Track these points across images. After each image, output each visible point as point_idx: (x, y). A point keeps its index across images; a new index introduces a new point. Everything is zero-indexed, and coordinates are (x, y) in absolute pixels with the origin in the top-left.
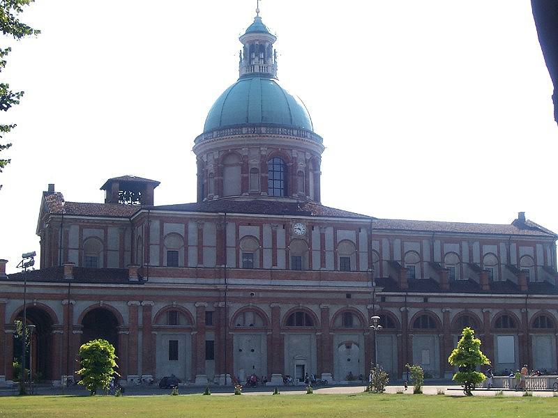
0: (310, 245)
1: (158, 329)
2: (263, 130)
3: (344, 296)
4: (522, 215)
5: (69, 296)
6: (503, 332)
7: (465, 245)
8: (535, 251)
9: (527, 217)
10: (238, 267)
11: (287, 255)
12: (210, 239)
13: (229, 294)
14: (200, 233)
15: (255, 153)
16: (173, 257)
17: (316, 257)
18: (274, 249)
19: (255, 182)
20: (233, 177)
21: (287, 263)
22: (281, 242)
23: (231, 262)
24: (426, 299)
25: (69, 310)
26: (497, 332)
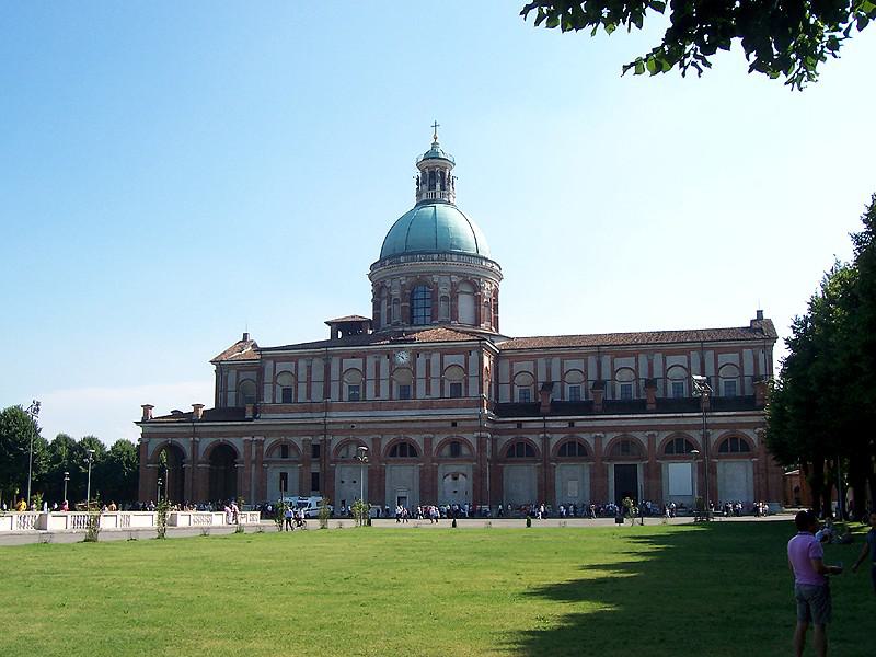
0: (414, 373)
1: (267, 462)
2: (402, 259)
3: (450, 425)
4: (760, 313)
5: (194, 435)
6: (674, 458)
7: (541, 362)
8: (741, 359)
9: (766, 316)
10: (341, 400)
11: (391, 386)
12: (318, 374)
13: (329, 427)
14: (309, 368)
15: (396, 283)
16: (287, 395)
17: (421, 385)
18: (378, 381)
19: (397, 310)
20: (384, 310)
21: (391, 393)
22: (385, 373)
23: (334, 396)
24: (572, 423)
25: (195, 445)
26: (663, 459)
